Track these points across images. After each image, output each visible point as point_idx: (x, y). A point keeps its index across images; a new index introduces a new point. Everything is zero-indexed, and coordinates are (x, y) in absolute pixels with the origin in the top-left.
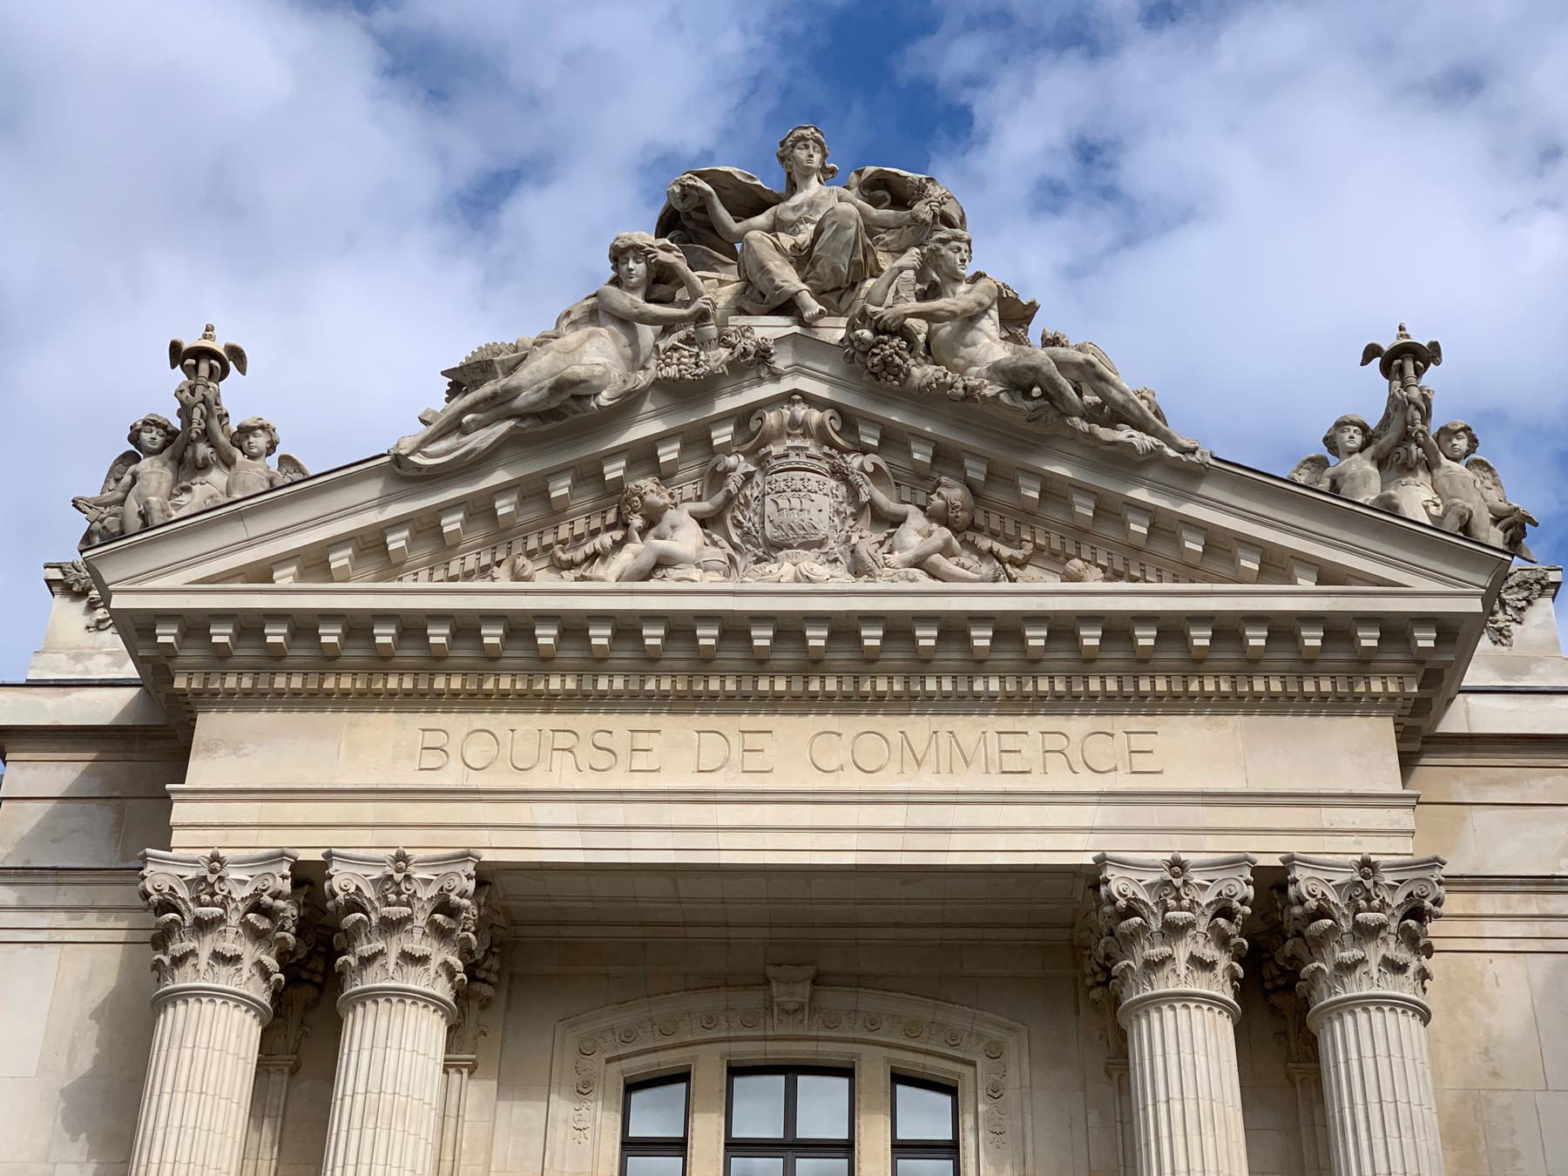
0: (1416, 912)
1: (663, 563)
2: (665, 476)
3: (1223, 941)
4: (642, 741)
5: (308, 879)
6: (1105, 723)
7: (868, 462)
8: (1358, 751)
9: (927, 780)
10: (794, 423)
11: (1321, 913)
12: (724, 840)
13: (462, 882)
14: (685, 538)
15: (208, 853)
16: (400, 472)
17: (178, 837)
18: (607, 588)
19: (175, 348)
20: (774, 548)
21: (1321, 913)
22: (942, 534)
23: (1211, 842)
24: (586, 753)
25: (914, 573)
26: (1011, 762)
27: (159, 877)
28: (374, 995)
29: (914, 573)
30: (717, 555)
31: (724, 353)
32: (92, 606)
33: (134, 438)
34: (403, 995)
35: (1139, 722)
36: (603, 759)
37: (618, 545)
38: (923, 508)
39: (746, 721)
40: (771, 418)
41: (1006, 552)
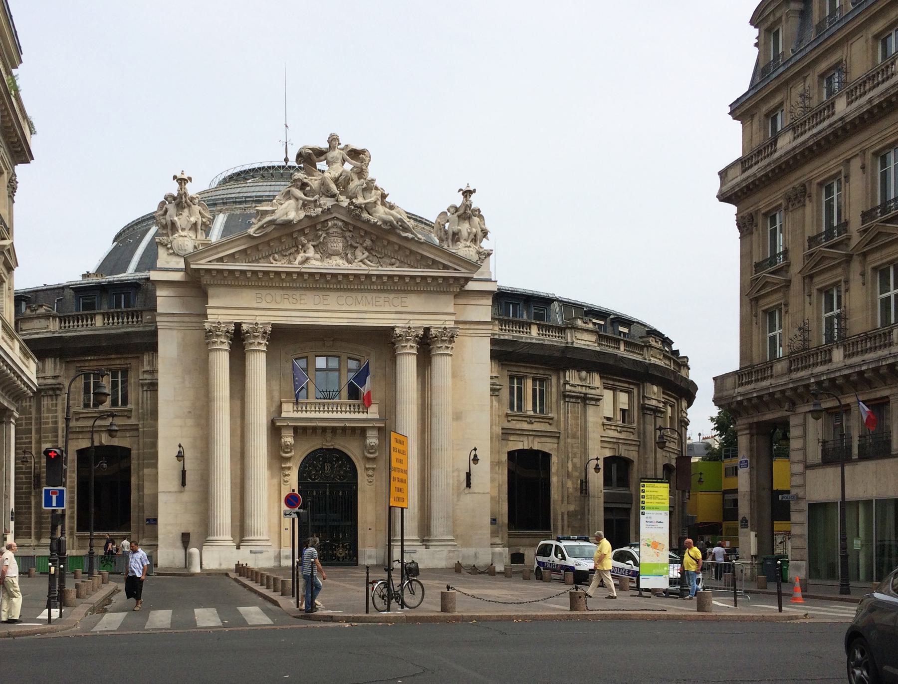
0: (453, 337)
1: (307, 259)
2: (305, 235)
3: (416, 342)
4: (303, 297)
5: (238, 326)
6: (396, 295)
7: (350, 234)
8: (447, 305)
9: (361, 308)
10: (335, 225)
12: (320, 320)
13: (269, 328)
14: (311, 252)
17: (209, 317)
18: (295, 264)
19: (175, 177)
20: (330, 256)
22: (367, 254)
24: (291, 299)
25: (360, 264)
26: (378, 304)
27: (207, 326)
28: (254, 350)
29: (360, 264)
30: (318, 256)
31: (320, 209)
32: (168, 249)
33: (166, 199)
34: (259, 351)
35: (403, 295)
36: (295, 301)
37: (297, 252)
39: (324, 293)
40: (330, 224)
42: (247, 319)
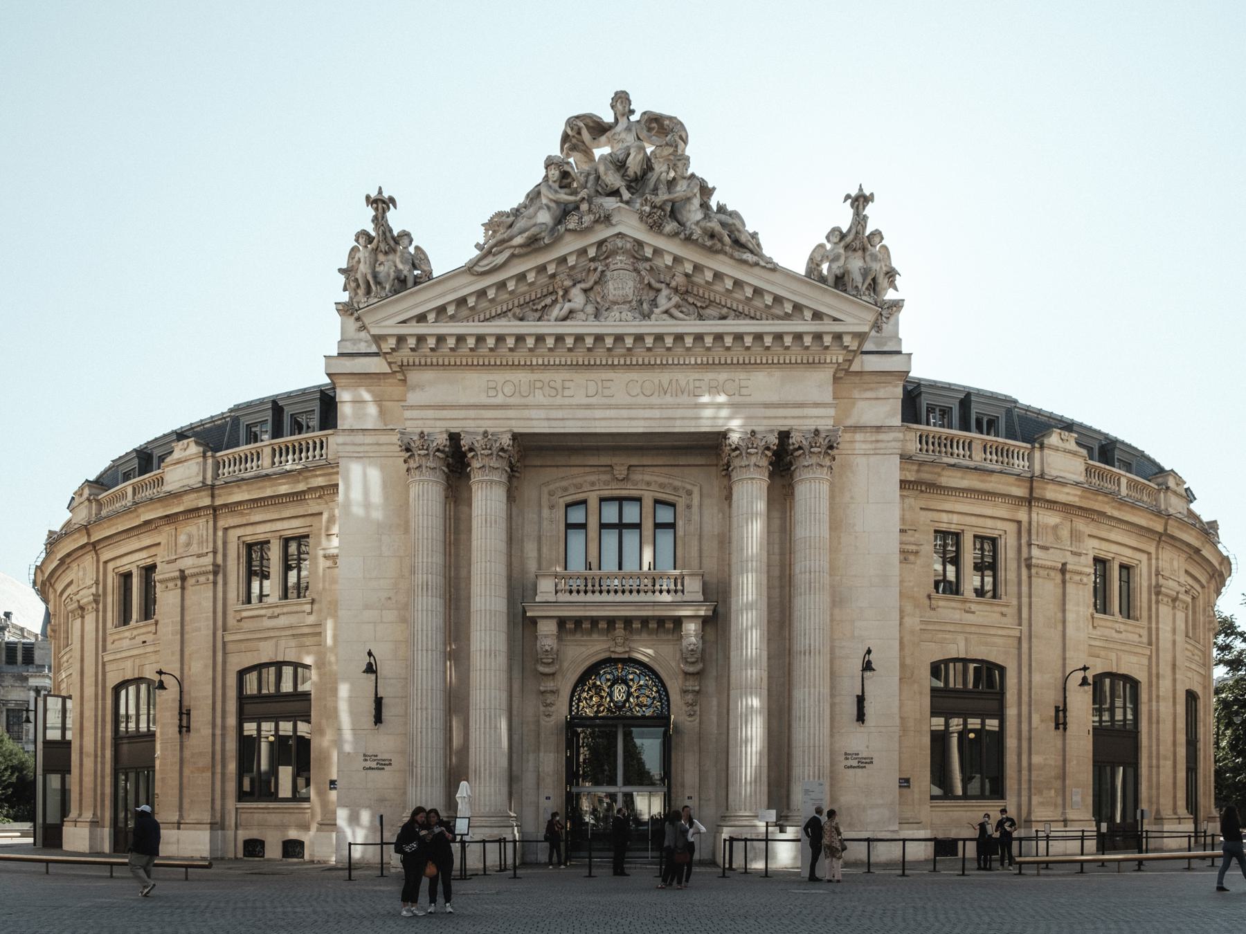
1: (570, 315)
11: (800, 448)
15: (419, 430)
16: (470, 269)
21: (800, 448)
22: (676, 299)
23: (765, 422)
36: (553, 393)
37: (555, 302)
38: (668, 285)
41: (699, 304)
42: (471, 425)
